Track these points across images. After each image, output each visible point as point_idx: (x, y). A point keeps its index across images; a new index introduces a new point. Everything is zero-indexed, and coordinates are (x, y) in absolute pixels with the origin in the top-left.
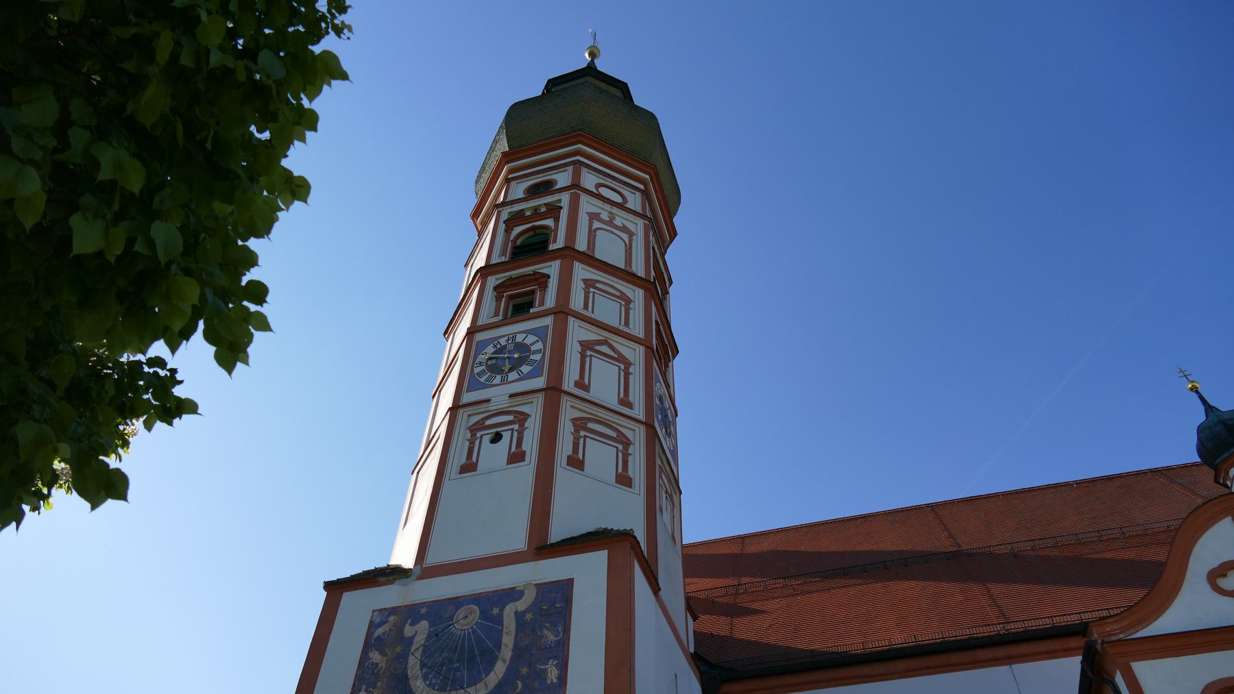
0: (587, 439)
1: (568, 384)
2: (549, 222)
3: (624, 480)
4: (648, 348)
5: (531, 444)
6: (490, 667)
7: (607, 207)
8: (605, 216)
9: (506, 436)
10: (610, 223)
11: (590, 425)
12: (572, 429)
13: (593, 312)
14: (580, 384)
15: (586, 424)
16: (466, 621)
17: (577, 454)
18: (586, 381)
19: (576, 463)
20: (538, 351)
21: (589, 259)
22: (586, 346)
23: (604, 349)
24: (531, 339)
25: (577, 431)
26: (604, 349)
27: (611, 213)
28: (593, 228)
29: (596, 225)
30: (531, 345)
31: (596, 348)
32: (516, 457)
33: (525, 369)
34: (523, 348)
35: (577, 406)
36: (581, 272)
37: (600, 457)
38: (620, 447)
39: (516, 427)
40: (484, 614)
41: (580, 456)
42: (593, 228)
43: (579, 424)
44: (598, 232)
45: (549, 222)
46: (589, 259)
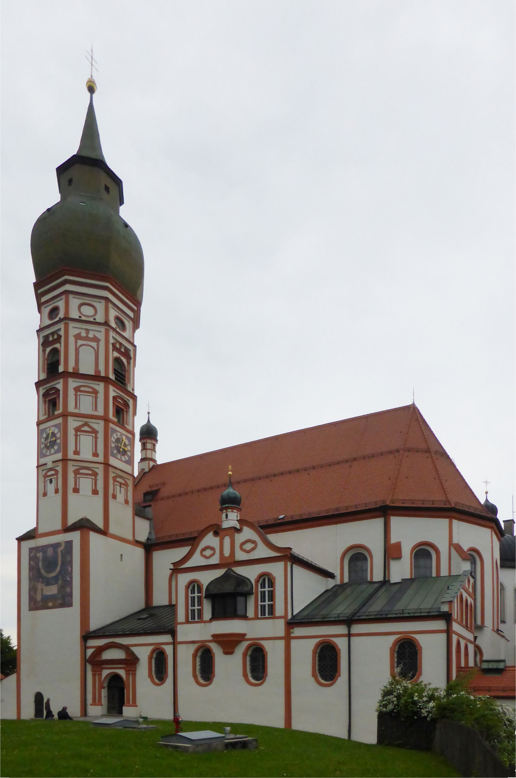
0: (80, 478)
1: (71, 455)
2: (57, 346)
3: (95, 492)
4: (106, 419)
5: (60, 486)
6: (56, 568)
7: (85, 326)
8: (83, 334)
9: (53, 480)
10: (87, 338)
11: (81, 471)
12: (74, 476)
13: (80, 409)
14: (77, 453)
15: (79, 471)
16: (50, 552)
17: (77, 487)
18: (78, 450)
19: (76, 490)
20: (59, 438)
21: (76, 375)
22: (77, 430)
23: (86, 428)
24: (56, 431)
25: (76, 476)
26: (86, 428)
27: (86, 329)
28: (78, 346)
29: (80, 342)
30: (57, 433)
31: (83, 429)
32: (57, 491)
33: (56, 447)
34: (53, 434)
35: (74, 464)
36: (73, 383)
37: (86, 484)
38: (93, 477)
39: (55, 477)
40: (54, 551)
41: (78, 487)
42: (78, 346)
43: (76, 472)
44: (81, 349)
45: (57, 346)
46: (76, 375)
